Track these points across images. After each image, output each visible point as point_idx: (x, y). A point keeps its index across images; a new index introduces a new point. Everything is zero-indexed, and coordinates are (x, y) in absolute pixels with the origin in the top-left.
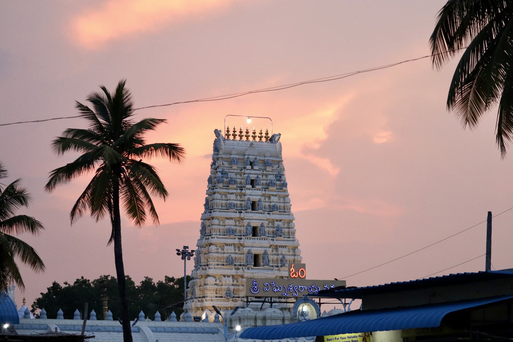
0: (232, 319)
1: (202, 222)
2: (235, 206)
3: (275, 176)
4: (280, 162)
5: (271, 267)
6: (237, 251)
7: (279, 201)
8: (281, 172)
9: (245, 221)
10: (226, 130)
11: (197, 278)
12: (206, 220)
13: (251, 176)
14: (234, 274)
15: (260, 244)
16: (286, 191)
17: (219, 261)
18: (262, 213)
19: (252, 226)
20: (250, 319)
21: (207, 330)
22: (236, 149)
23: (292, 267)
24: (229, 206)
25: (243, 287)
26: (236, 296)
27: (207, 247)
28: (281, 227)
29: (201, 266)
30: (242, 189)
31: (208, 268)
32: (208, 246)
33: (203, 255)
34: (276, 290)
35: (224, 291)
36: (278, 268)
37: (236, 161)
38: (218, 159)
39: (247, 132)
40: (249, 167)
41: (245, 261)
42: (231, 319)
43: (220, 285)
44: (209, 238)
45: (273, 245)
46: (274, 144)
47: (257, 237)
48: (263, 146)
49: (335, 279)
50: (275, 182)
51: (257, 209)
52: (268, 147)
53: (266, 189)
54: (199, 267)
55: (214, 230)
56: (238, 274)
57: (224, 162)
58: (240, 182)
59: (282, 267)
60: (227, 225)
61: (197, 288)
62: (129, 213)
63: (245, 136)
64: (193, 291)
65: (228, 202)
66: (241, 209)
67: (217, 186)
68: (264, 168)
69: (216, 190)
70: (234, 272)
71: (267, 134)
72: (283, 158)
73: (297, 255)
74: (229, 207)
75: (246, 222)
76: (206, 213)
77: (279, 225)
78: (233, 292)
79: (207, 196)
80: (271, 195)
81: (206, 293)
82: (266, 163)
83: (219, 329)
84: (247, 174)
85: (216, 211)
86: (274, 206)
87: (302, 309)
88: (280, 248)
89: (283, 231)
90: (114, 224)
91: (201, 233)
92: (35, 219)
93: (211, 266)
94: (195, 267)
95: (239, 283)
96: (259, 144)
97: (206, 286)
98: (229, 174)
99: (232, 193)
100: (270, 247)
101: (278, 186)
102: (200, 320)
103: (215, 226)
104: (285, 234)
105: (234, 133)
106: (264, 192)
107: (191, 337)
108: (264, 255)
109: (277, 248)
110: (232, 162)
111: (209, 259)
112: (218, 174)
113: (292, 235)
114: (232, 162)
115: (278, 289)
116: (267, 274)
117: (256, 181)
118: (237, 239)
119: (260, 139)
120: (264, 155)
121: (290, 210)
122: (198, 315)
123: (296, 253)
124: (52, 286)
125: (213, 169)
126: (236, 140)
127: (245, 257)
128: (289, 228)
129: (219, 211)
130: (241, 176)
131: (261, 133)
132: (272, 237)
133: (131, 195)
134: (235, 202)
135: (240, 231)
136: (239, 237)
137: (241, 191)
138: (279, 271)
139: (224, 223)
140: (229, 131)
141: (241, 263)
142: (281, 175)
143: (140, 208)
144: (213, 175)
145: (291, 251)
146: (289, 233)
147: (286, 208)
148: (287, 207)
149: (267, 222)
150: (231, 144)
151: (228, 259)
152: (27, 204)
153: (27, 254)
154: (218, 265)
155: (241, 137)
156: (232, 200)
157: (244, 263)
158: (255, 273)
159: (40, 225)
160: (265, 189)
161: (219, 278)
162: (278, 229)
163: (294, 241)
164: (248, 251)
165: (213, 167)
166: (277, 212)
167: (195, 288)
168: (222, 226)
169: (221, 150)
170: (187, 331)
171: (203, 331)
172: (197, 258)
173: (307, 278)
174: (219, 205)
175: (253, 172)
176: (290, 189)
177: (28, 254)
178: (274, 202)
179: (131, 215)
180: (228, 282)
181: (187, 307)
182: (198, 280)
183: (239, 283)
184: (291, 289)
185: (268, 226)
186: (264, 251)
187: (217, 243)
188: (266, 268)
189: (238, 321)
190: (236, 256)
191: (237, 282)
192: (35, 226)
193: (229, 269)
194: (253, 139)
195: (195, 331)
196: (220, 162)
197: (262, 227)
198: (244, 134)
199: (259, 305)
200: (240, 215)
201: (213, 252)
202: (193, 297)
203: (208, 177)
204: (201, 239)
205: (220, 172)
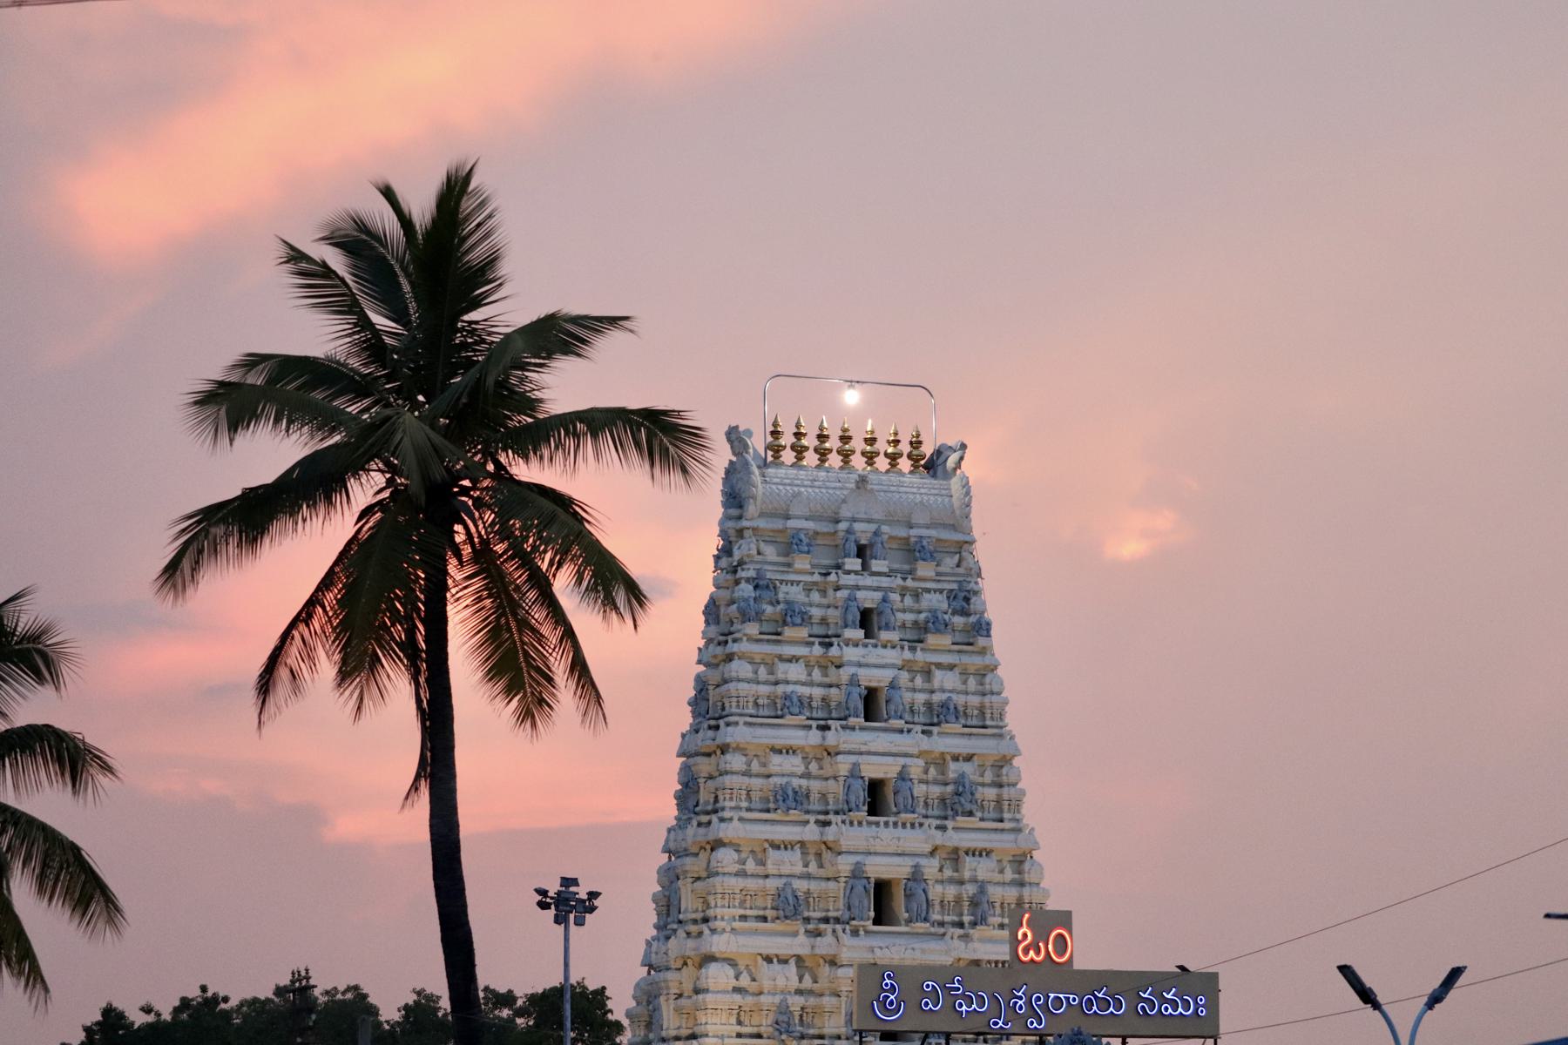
1: (683, 763)
2: (804, 703)
3: (948, 598)
4: (963, 547)
5: (936, 924)
7: (963, 687)
8: (970, 582)
9: (840, 758)
10: (770, 428)
11: (668, 969)
12: (697, 754)
13: (860, 595)
16: (988, 652)
17: (748, 906)
18: (901, 731)
19: (866, 779)
22: (808, 498)
23: (1022, 925)
24: (784, 704)
25: (837, 998)
26: (811, 1031)
27: (703, 856)
28: (973, 783)
29: (680, 922)
30: (831, 645)
31: (707, 932)
32: (709, 850)
34: (964, 1008)
35: (767, 1015)
36: (960, 931)
37: (806, 540)
38: (740, 533)
39: (845, 439)
40: (854, 563)
41: (841, 904)
44: (709, 823)
45: (944, 846)
46: (941, 482)
47: (885, 819)
49: (1179, 967)
50: (946, 617)
51: (886, 716)
52: (922, 491)
53: (914, 644)
54: (675, 926)
55: (729, 791)
56: (817, 951)
57: (762, 545)
58: (822, 620)
59: (978, 927)
60: (777, 775)
61: (668, 1006)
62: (490, 679)
63: (838, 452)
64: (651, 1017)
65: (780, 689)
66: (825, 716)
67: (739, 631)
68: (906, 567)
69: (733, 648)
70: (802, 945)
71: (916, 444)
72: (976, 533)
73: (1030, 884)
74: (781, 708)
75: (843, 765)
77: (963, 775)
78: (801, 1016)
79: (702, 668)
80: (933, 667)
81: (703, 1022)
82: (914, 551)
84: (846, 587)
85: (737, 723)
86: (944, 705)
88: (968, 859)
89: (978, 796)
90: (428, 723)
91: (677, 805)
92: (86, 740)
93: (719, 924)
94: (657, 927)
95: (823, 984)
96: (890, 481)
97: (700, 997)
98: (783, 588)
99: (794, 656)
100: (932, 853)
101: (957, 634)
103: (735, 777)
104: (986, 807)
105: (799, 439)
106: (907, 655)
108: (910, 884)
109: (957, 859)
110: (792, 543)
111: (711, 899)
113: (1009, 809)
114: (791, 544)
115: (974, 1006)
116: (923, 951)
117: (880, 613)
118: (812, 827)
119: (890, 464)
120: (905, 519)
121: (1001, 719)
123: (1026, 875)
124: (101, 1019)
125: (722, 570)
126: (805, 466)
127: (842, 891)
128: (1001, 786)
129: (746, 724)
130: (825, 597)
131: (896, 442)
132: (938, 818)
133: (500, 610)
135: (824, 795)
136: (821, 817)
137: (827, 649)
138: (967, 943)
139: (764, 765)
140: (778, 433)
141: (828, 910)
142: (969, 591)
143: (534, 660)
144: (725, 594)
145: (1008, 866)
146: (999, 802)
147: (989, 711)
148: (992, 707)
149: (921, 762)
150: (788, 481)
151: (779, 896)
152: (59, 682)
153: (56, 865)
154: (743, 918)
155: (823, 454)
156: (796, 683)
157: (841, 913)
158: (881, 948)
159: (104, 763)
160: (910, 644)
161: (747, 965)
162: (961, 789)
163: (1018, 830)
164: (852, 867)
165: (724, 562)
166: (957, 728)
167: (659, 1004)
168: (758, 776)
169: (751, 501)
172: (667, 893)
173: (1077, 965)
174: (747, 702)
175: (868, 581)
176: (1001, 641)
177: (61, 868)
178: (944, 691)
179: (500, 685)
180: (781, 982)
182: (670, 975)
183: (823, 984)
184: (1020, 1002)
185: (924, 777)
186: (909, 870)
187: (739, 838)
188: (921, 931)
190: (811, 888)
191: (816, 982)
192: (83, 765)
193: (783, 934)
194: (866, 463)
196: (749, 543)
197: (903, 779)
198: (833, 443)
200: (824, 738)
201: (726, 870)
202: (651, 1036)
203: (705, 599)
204: (682, 823)
205: (748, 580)
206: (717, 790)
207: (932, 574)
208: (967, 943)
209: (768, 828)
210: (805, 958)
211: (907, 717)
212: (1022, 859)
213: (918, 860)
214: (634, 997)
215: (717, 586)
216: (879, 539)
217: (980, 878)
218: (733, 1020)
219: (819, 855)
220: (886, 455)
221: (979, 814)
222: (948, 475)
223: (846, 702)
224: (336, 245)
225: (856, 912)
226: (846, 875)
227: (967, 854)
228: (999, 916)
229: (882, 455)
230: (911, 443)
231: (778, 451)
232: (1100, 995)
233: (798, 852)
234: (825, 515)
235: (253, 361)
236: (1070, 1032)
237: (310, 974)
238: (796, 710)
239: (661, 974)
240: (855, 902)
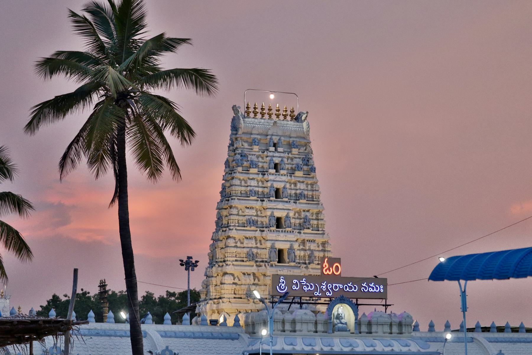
0: (255, 323)
2: (256, 193)
3: (302, 160)
4: (307, 145)
6: (259, 245)
11: (212, 277)
12: (222, 209)
13: (274, 159)
14: (255, 272)
15: (285, 237)
16: (315, 178)
18: (287, 202)
19: (276, 217)
20: (277, 322)
21: (225, 335)
22: (258, 128)
23: (324, 262)
25: (266, 286)
27: (224, 241)
29: (216, 262)
30: (265, 174)
31: (225, 265)
32: (226, 239)
33: (219, 251)
36: (305, 266)
37: (257, 141)
39: (270, 110)
40: (272, 149)
41: (267, 256)
42: (254, 323)
43: (239, 285)
44: (226, 230)
47: (281, 229)
48: (288, 126)
49: (374, 276)
55: (232, 220)
57: (244, 144)
58: (262, 167)
63: (268, 114)
65: (249, 188)
66: (263, 197)
68: (289, 150)
69: (234, 175)
70: (255, 269)
72: (311, 140)
75: (269, 213)
76: (222, 202)
79: (224, 182)
82: (291, 145)
83: (240, 334)
85: (235, 199)
86: (300, 194)
87: (338, 310)
91: (216, 225)
93: (228, 263)
94: (209, 264)
97: (222, 285)
100: (297, 241)
102: (217, 323)
106: (289, 177)
107: (208, 343)
108: (289, 250)
109: (304, 243)
112: (237, 157)
117: (280, 165)
118: (258, 231)
119: (284, 118)
122: (214, 317)
123: (326, 248)
127: (268, 253)
128: (318, 220)
130: (263, 159)
131: (286, 111)
132: (298, 229)
134: (257, 189)
136: (262, 229)
138: (307, 269)
139: (243, 212)
140: (249, 107)
142: (309, 158)
144: (231, 159)
146: (318, 225)
151: (248, 254)
154: (236, 261)
155: (263, 115)
162: (306, 220)
164: (271, 245)
165: (231, 148)
166: (305, 201)
167: (209, 288)
168: (241, 215)
169: (240, 129)
170: (202, 336)
171: (221, 337)
175: (277, 154)
180: (248, 282)
181: (200, 310)
182: (213, 279)
184: (324, 287)
185: (294, 217)
188: (293, 265)
189: (262, 324)
195: (212, 337)
198: (266, 111)
199: (284, 308)
201: (231, 245)
203: (225, 160)
204: (217, 231)
205: (239, 154)
206: (228, 220)
207: (297, 153)
208: (307, 269)
209: (244, 232)
210: (255, 273)
211: (289, 197)
212: (325, 243)
213: (292, 243)
214: (202, 286)
215: (229, 156)
216: (280, 141)
217: (312, 249)
218: (233, 292)
219: (260, 241)
220: (283, 115)
221: (311, 229)
222: (302, 122)
223: (270, 193)
224: (88, 12)
225: (272, 259)
226: (269, 247)
227: (307, 241)
228: (317, 261)
229: (281, 115)
230: (291, 111)
231: (249, 113)
232: (350, 285)
234: (263, 133)
235: (59, 53)
236: (340, 297)
237: (106, 281)
238: (253, 195)
239: (210, 279)
240: (272, 256)
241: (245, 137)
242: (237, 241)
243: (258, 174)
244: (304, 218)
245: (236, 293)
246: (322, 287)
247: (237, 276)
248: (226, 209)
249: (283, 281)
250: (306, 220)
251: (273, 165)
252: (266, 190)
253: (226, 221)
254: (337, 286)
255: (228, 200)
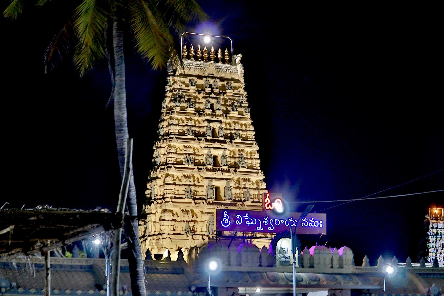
11: (151, 213)
12: (160, 147)
36: (241, 203)
41: (205, 194)
47: (218, 167)
48: (222, 68)
68: (224, 91)
78: (193, 228)
85: (173, 138)
108: (226, 188)
118: (196, 169)
154: (175, 198)
167: (148, 225)
180: (187, 219)
191: (197, 217)
206: (167, 158)
217: (247, 187)
218: (172, 229)
219: (198, 179)
222: (235, 64)
233: (192, 179)
241: (182, 79)
242: (175, 178)
243: (195, 114)
244: (239, 157)
245: (175, 229)
246: (265, 222)
247: (176, 213)
248: (164, 147)
249: (227, 216)
250: (241, 159)
251: (209, 106)
252: (202, 130)
253: (164, 159)
254: (278, 221)
255: (166, 139)
